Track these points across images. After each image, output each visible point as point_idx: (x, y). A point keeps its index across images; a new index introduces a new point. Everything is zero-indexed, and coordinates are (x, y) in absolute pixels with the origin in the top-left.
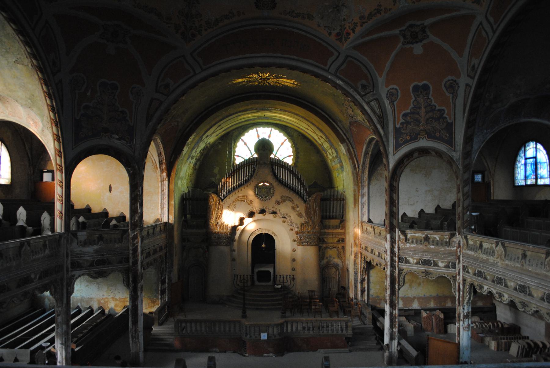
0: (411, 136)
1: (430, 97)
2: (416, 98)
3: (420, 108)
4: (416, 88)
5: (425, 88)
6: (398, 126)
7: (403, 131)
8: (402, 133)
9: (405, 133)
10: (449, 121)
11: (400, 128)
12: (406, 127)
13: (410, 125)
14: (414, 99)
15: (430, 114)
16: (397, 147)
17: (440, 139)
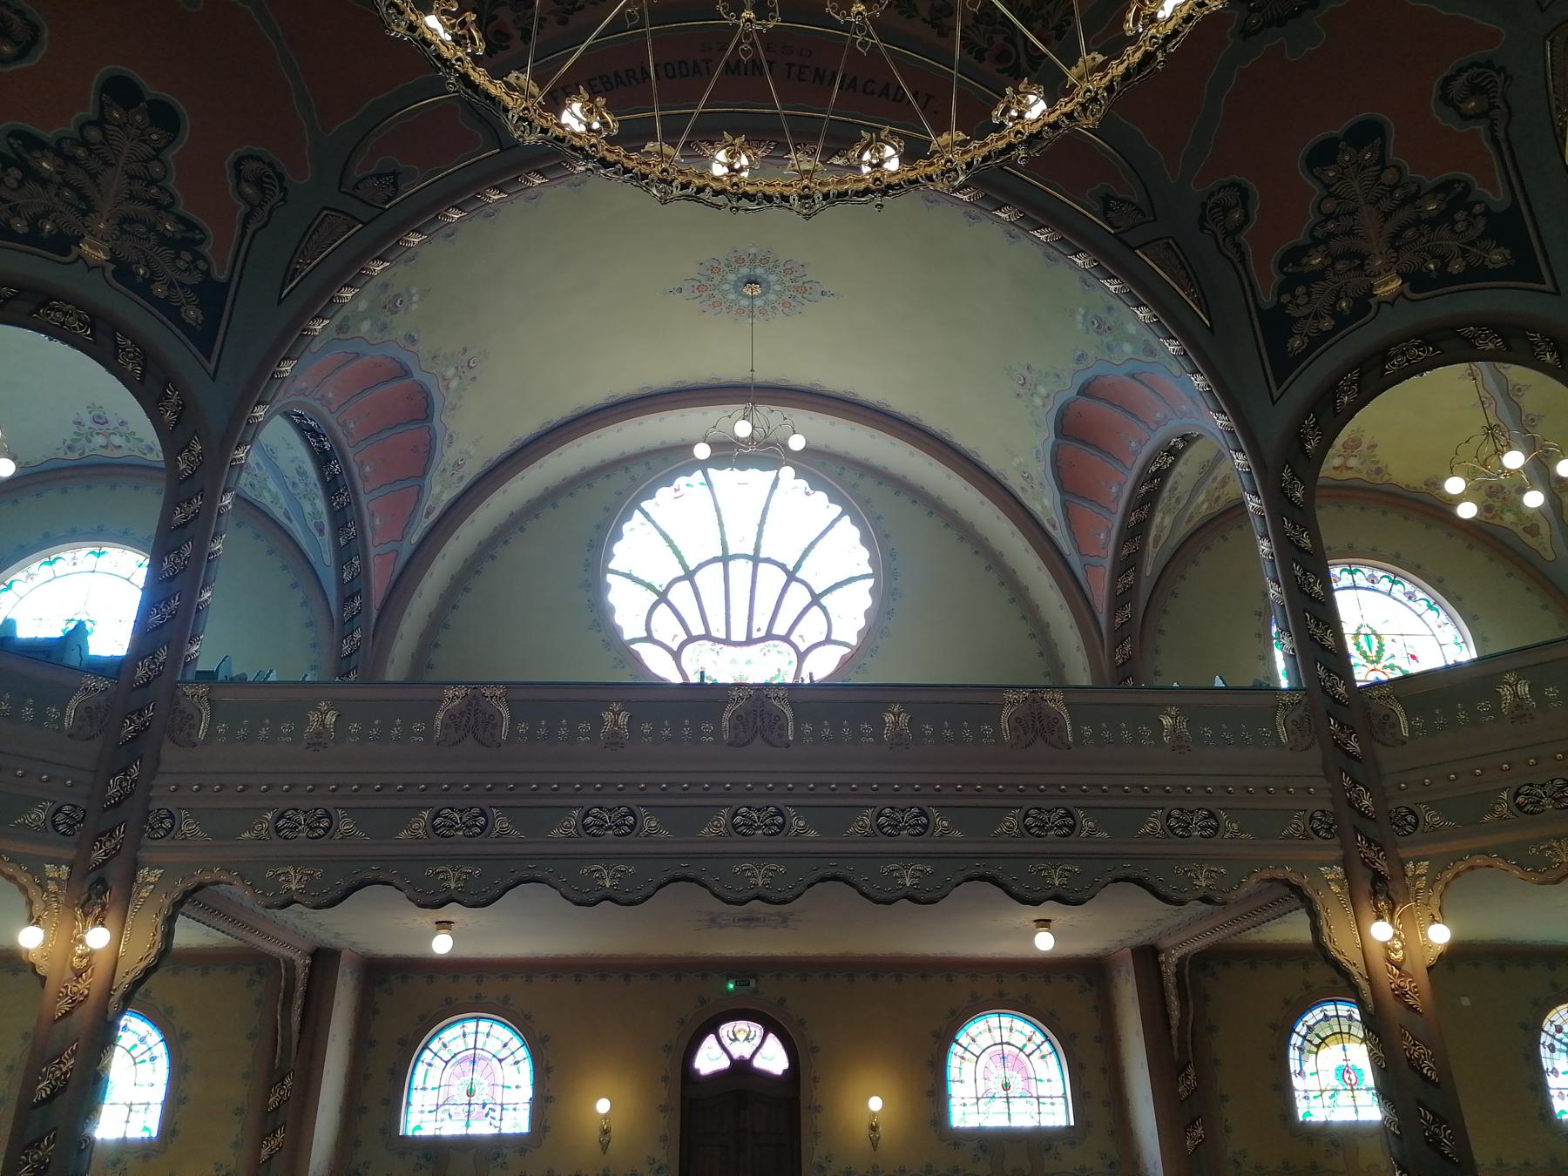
0: (1336, 314)
1: (1391, 157)
2: (1327, 186)
3: (1351, 213)
4: (1323, 155)
5: (1365, 134)
6: (1267, 300)
7: (1295, 313)
8: (1296, 320)
9: (1306, 317)
10: (1498, 199)
11: (1280, 307)
12: (1308, 294)
13: (1324, 280)
14: (1318, 191)
15: (1405, 214)
16: (1283, 366)
17: (1476, 274)
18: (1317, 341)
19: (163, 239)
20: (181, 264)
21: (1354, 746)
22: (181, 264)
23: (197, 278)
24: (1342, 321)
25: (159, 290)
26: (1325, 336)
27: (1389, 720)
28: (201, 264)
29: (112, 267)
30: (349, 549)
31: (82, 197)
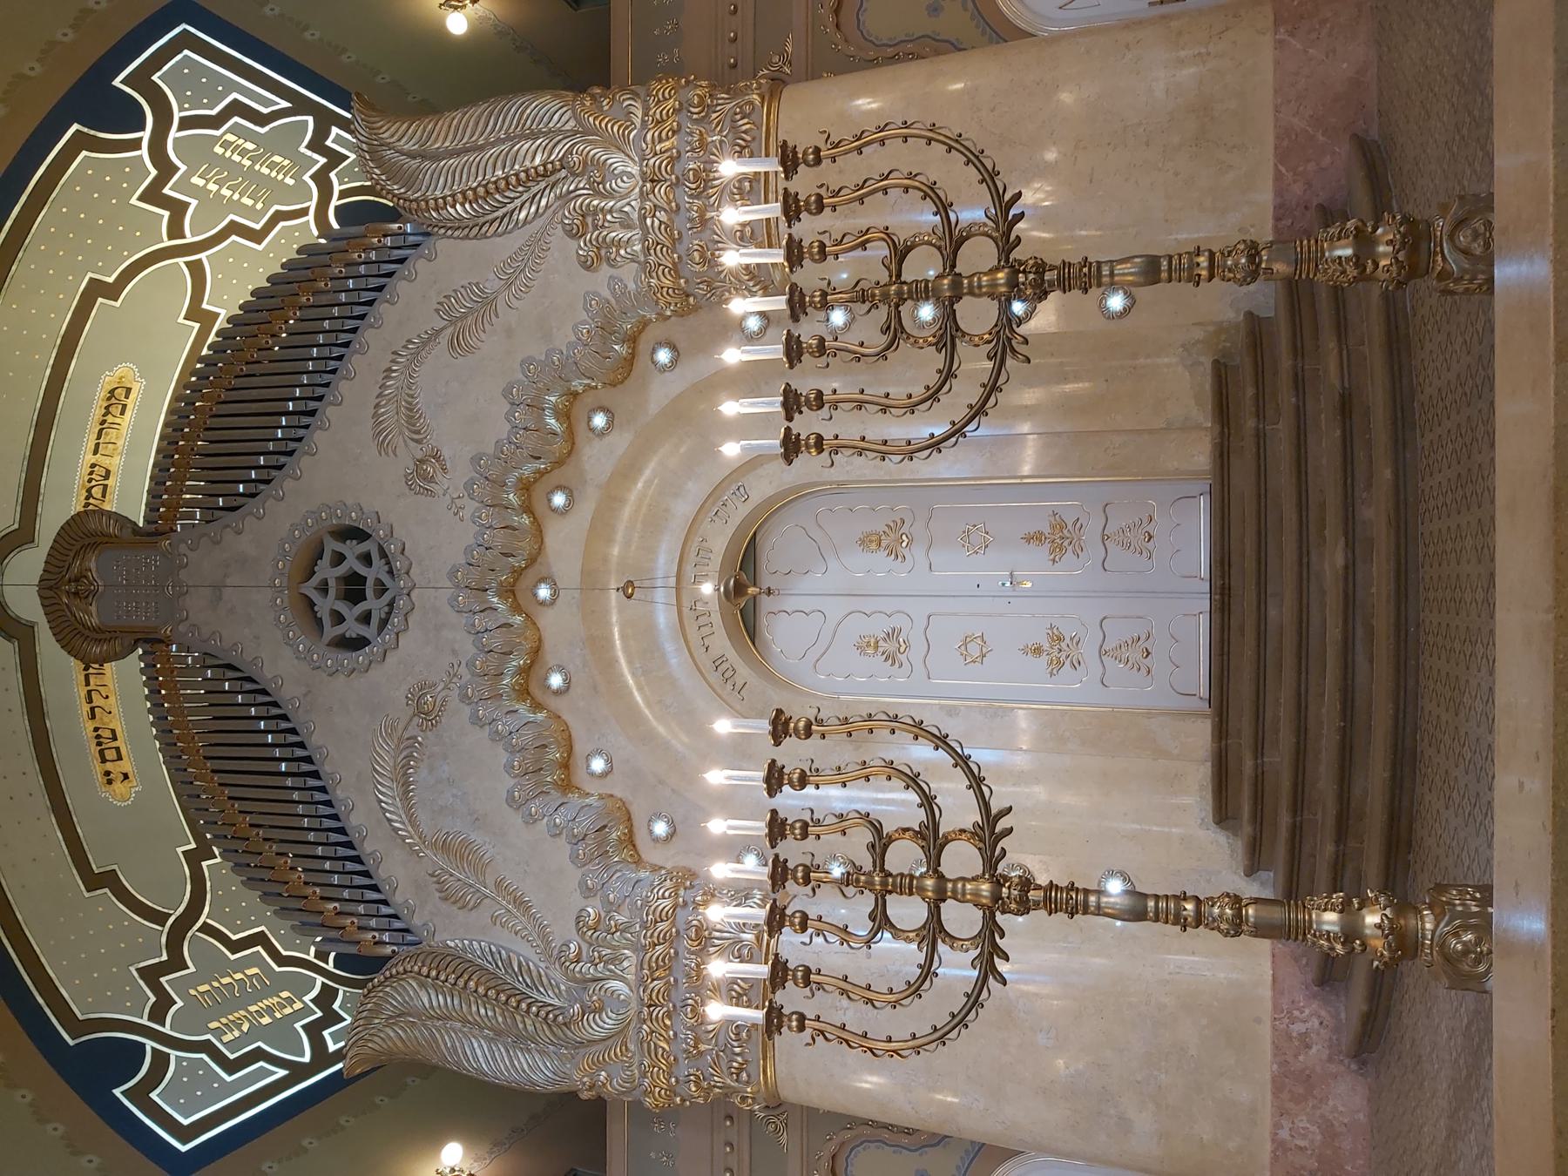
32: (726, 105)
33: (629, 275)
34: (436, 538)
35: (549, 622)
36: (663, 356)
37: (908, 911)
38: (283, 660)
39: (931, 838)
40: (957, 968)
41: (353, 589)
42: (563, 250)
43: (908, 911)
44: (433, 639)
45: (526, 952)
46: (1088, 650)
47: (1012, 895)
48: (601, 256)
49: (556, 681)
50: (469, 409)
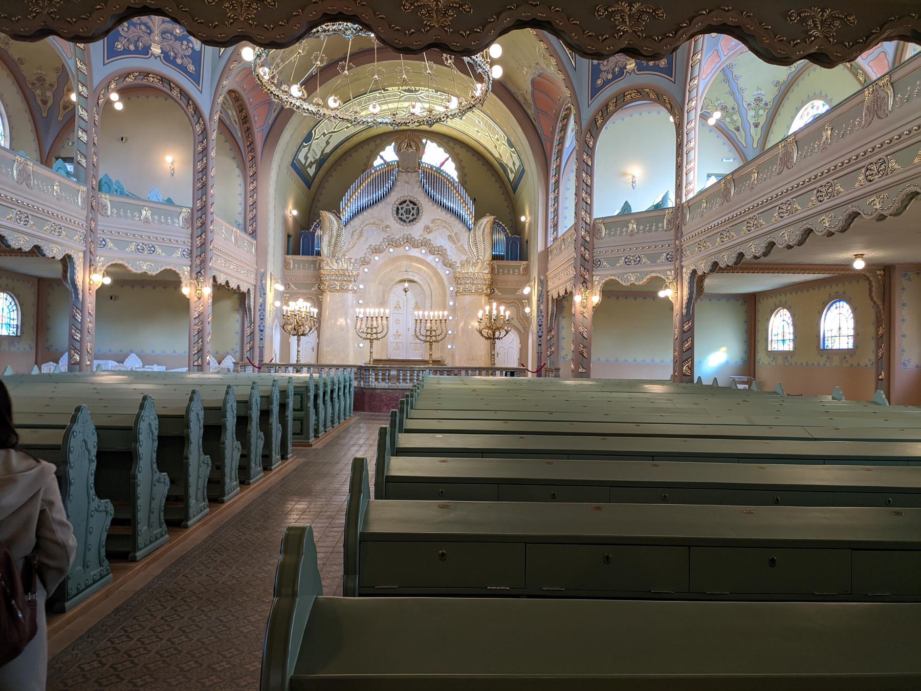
0: (613, 73)
16: (595, 91)
18: (606, 83)
19: (177, 38)
20: (184, 47)
21: (588, 239)
22: (184, 47)
23: (189, 52)
24: (615, 77)
25: (179, 61)
26: (609, 81)
27: (600, 231)
28: (191, 45)
29: (162, 56)
30: (248, 132)
31: (148, 27)
32: (485, 287)
33: (459, 270)
34: (416, 231)
35: (402, 248)
36: (447, 272)
37: (369, 331)
38: (394, 198)
39: (376, 333)
40: (364, 335)
41: (408, 212)
42: (464, 258)
43: (369, 331)
44: (398, 229)
45: (345, 248)
46: (397, 340)
47: (371, 341)
48: (462, 265)
49: (391, 250)
50: (439, 239)
